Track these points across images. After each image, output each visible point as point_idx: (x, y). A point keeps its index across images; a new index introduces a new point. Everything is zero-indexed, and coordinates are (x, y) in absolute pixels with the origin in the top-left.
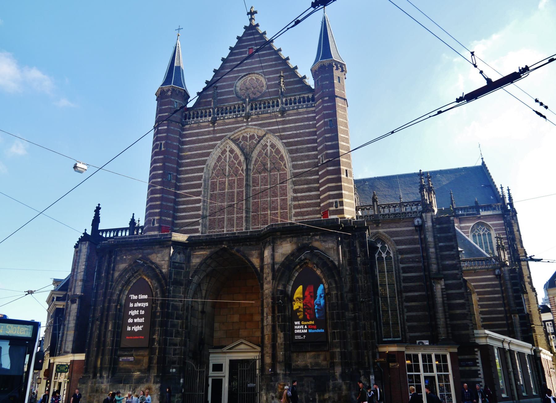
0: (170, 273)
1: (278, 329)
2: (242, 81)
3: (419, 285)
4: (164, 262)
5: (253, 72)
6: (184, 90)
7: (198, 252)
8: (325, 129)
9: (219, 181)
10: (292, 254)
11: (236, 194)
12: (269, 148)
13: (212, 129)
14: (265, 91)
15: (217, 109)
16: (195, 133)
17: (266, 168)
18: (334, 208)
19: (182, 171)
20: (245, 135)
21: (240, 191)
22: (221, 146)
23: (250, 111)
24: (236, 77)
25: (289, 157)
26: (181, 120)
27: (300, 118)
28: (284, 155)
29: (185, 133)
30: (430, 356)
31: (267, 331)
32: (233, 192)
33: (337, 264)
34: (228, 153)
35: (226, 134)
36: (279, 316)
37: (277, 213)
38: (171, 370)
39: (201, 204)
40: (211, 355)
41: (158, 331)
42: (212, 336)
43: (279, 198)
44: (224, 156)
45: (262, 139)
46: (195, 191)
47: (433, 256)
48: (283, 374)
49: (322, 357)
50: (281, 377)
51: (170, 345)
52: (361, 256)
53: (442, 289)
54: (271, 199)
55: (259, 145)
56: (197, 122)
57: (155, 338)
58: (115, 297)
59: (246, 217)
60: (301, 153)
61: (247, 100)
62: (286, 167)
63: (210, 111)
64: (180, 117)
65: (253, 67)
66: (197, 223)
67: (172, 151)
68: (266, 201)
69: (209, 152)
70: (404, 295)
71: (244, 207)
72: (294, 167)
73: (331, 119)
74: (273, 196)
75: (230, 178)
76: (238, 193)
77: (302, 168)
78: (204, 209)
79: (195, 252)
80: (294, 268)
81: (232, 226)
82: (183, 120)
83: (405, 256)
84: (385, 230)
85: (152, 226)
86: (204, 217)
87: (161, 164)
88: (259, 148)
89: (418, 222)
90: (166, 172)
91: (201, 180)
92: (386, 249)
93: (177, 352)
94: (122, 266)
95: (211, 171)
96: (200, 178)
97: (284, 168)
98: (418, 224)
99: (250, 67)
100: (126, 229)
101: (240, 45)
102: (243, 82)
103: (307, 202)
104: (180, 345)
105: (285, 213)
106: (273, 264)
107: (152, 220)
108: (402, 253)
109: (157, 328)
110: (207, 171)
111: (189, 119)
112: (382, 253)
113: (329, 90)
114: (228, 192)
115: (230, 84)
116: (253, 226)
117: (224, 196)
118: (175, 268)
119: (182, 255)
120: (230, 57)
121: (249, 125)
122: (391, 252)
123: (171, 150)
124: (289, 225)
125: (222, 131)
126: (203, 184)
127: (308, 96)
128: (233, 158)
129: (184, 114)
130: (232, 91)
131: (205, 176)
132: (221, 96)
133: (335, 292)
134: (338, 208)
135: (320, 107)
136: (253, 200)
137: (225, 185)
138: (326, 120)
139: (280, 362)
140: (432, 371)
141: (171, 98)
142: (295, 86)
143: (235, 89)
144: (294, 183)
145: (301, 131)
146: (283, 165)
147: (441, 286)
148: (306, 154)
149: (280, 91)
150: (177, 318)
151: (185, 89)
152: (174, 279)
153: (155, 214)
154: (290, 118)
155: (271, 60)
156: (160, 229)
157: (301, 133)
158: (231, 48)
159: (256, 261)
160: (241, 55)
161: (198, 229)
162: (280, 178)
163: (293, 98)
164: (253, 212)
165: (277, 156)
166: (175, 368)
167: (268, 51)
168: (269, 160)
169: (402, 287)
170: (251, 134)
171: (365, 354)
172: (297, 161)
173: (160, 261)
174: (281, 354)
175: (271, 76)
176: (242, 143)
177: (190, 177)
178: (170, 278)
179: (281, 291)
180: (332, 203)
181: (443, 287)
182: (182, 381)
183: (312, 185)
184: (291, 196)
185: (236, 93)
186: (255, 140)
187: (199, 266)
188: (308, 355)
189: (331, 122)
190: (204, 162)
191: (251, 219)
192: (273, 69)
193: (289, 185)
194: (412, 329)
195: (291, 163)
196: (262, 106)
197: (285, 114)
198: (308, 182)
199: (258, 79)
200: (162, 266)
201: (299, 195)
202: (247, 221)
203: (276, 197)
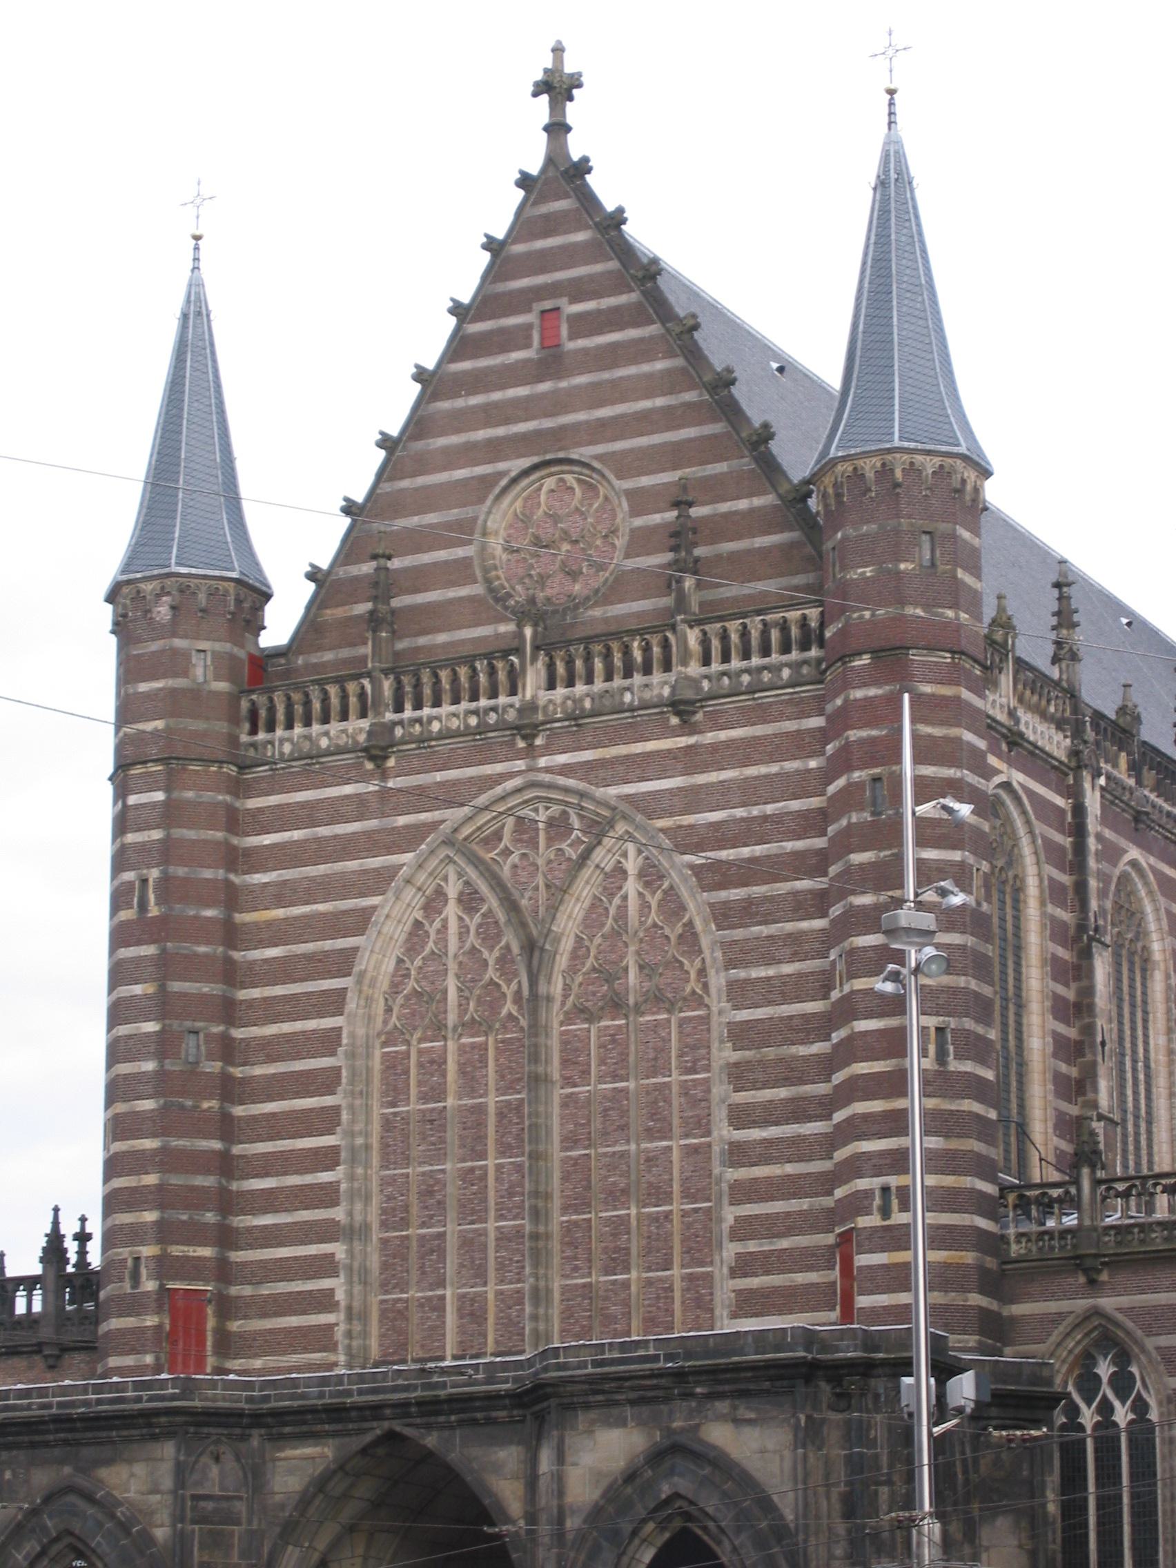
0: (181, 1539)
4: (158, 1497)
5: (561, 455)
7: (292, 1448)
9: (420, 1052)
11: (492, 1120)
12: (632, 886)
16: (303, 805)
20: (527, 812)
22: (421, 878)
23: (542, 693)
24: (486, 482)
26: (233, 740)
27: (765, 737)
28: (699, 925)
29: (253, 803)
32: (480, 1110)
34: (452, 910)
35: (436, 815)
37: (668, 1216)
44: (437, 924)
46: (311, 1110)
52: (896, 1478)
54: (643, 1146)
55: (586, 873)
60: (765, 923)
62: (705, 986)
64: (222, 727)
66: (326, 1267)
68: (623, 1155)
69: (364, 909)
73: (877, 770)
74: (650, 1134)
75: (464, 1040)
76: (501, 1115)
77: (770, 1003)
79: (281, 1449)
80: (635, 1533)
81: (480, 1275)
82: (244, 738)
84: (1125, 1301)
85: (129, 1291)
88: (585, 888)
91: (333, 1054)
95: (382, 1001)
96: (328, 1042)
99: (548, 423)
100: (29, 1283)
101: (502, 287)
103: (790, 1169)
105: (700, 1216)
107: (130, 1263)
110: (362, 1002)
111: (271, 728)
113: (873, 615)
117: (443, 1128)
118: (202, 1519)
121: (539, 770)
122: (1152, 1402)
123: (192, 913)
125: (421, 798)
126: (344, 1073)
128: (478, 933)
129: (245, 705)
130: (466, 563)
131: (352, 1035)
132: (416, 591)
138: (856, 775)
141: (174, 634)
143: (483, 548)
144: (739, 1076)
145: (769, 809)
146: (693, 975)
148: (790, 927)
153: (135, 1235)
154: (723, 735)
155: (650, 386)
157: (765, 818)
158: (457, 309)
161: (332, 1291)
164: (565, 1209)
165: (667, 931)
170: (555, 809)
172: (747, 964)
173: (143, 1494)
175: (645, 481)
176: (514, 858)
177: (289, 1038)
180: (868, 1194)
187: (295, 1508)
189: (878, 785)
190: (343, 963)
191: (556, 1245)
192: (657, 439)
195: (722, 974)
196: (598, 665)
197: (699, 716)
198: (792, 1073)
200: (153, 1513)
201: (756, 1134)
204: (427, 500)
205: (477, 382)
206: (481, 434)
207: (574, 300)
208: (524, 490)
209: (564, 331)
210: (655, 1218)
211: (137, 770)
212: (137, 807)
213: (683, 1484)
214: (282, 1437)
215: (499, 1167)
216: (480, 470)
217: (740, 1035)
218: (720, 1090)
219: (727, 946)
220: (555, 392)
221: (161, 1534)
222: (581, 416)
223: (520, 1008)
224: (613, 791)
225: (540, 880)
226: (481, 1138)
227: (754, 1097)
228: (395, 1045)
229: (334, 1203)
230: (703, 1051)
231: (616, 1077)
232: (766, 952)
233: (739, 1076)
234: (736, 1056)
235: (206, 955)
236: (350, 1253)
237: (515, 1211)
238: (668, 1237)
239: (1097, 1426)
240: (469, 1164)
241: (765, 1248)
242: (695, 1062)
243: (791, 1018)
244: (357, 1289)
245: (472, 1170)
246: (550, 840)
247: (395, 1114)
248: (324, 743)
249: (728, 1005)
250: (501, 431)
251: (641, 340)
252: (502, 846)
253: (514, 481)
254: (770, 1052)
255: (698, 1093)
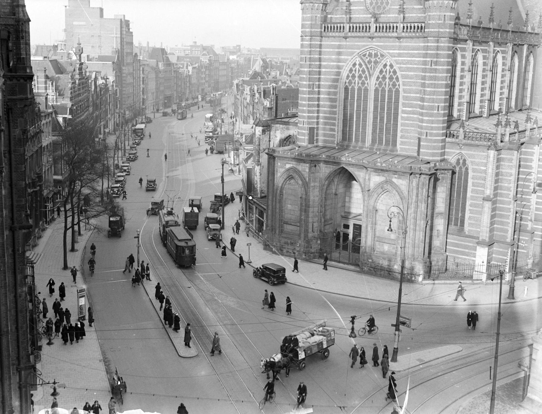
20: (371, 51)
28: (399, 76)
170: (376, 52)
229: (336, 108)
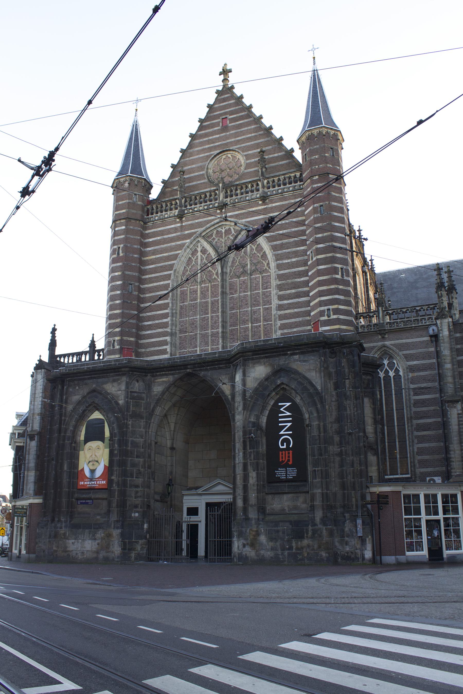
1: (250, 468)
2: (215, 161)
3: (434, 410)
4: (121, 392)
5: (228, 149)
6: (145, 179)
8: (314, 217)
9: (190, 289)
10: (267, 379)
11: (210, 305)
13: (179, 225)
14: (243, 171)
15: (184, 199)
16: (160, 231)
17: (246, 270)
18: (326, 318)
19: (146, 279)
20: (219, 229)
21: (215, 300)
25: (273, 255)
26: (143, 216)
27: (286, 204)
28: (267, 253)
29: (147, 232)
30: (435, 496)
31: (239, 470)
32: (207, 302)
33: (320, 389)
34: (199, 254)
35: (196, 230)
36: (251, 452)
37: (260, 326)
38: (133, 515)
39: (169, 319)
40: (185, 498)
41: (117, 472)
42: (186, 476)
43: (261, 307)
44: (195, 258)
45: (240, 234)
46: (162, 304)
47: (449, 374)
48: (255, 519)
49: (301, 499)
50: (253, 522)
51: (131, 486)
52: (350, 377)
53: (458, 414)
54: (252, 308)
56: (162, 217)
57: (114, 479)
58: (69, 434)
59: (223, 332)
60: (287, 249)
61: (221, 185)
62: (269, 268)
63: (176, 203)
64: (140, 212)
65: (227, 143)
66: (165, 343)
67: (132, 256)
68: (247, 311)
69: (176, 254)
70: (415, 422)
71: (220, 320)
72: (279, 267)
73: (321, 204)
74: (255, 305)
75: (203, 285)
76: (212, 303)
77: (289, 269)
78: (172, 325)
80: (269, 395)
81: (207, 344)
82: (145, 217)
83: (416, 374)
84: (393, 342)
85: (112, 349)
86: (172, 334)
87: (120, 273)
89: (433, 330)
90: (126, 282)
92: (394, 366)
93: (139, 494)
94: (76, 398)
95: (180, 277)
97: (267, 268)
98: (434, 333)
100: (86, 353)
101: (212, 114)
102: (216, 162)
103: (296, 310)
104: (142, 487)
106: (244, 391)
108: (414, 370)
109: (115, 468)
110: (175, 277)
112: (390, 371)
113: (318, 167)
114: (200, 303)
115: (201, 166)
116: (231, 343)
117: (196, 308)
118: (133, 398)
119: (141, 383)
120: (199, 131)
122: (401, 370)
123: (131, 255)
124: (262, 343)
125: (192, 227)
127: (295, 175)
128: (206, 259)
129: (146, 209)
130: (203, 174)
131: (173, 285)
132: (190, 183)
133: (317, 423)
134: (331, 318)
135: (309, 189)
136: (231, 311)
137: (197, 294)
138: (315, 205)
139: (252, 506)
140: (436, 513)
142: (281, 163)
143: (207, 172)
144: (280, 287)
146: (266, 265)
147: (458, 410)
148: (294, 249)
149: (260, 171)
150: (137, 457)
151: (145, 177)
152: (133, 411)
153: (115, 334)
154: (274, 205)
156: (121, 351)
157: (286, 223)
159: (226, 389)
160: (212, 128)
162: (262, 281)
163: (276, 179)
165: (258, 254)
166: (138, 512)
167: (246, 120)
168: (249, 260)
169: (412, 412)
171: (353, 495)
172: (282, 259)
173: (116, 391)
174: (253, 496)
175: (250, 152)
176: (216, 240)
177: (155, 287)
178: (128, 410)
179: (254, 423)
180: (324, 311)
181: (460, 412)
182: (146, 526)
183: (301, 289)
184: (276, 304)
185: (208, 177)
186: (231, 236)
187: (160, 395)
188: (285, 497)
189: (321, 207)
190: (171, 267)
192: (253, 143)
193: (273, 291)
194: (423, 463)
195: (275, 262)
197: (267, 201)
198: (296, 285)
199: (235, 157)
200: (119, 396)
201: (286, 302)
202: (223, 338)
203: (258, 306)
204: (193, 162)
205: (206, 135)
206: (207, 146)
207: (230, 115)
208: (217, 159)
209: (228, 122)
210: (256, 327)
211: (118, 222)
212: (118, 230)
213: (285, 380)
214: (157, 376)
215: (212, 317)
216: (206, 154)
217: (280, 277)
218: (274, 292)
219: (275, 255)
220: (225, 135)
221: (121, 402)
222: (233, 140)
223: (218, 277)
224: (244, 220)
225: (223, 245)
226: (207, 309)
227: (285, 292)
228: (184, 288)
230: (269, 284)
231: (245, 292)
232: (288, 256)
233: (280, 287)
234: (279, 283)
235: (134, 266)
236: (171, 339)
237: (216, 327)
238: (260, 331)
239: (384, 377)
240: (204, 316)
241: (290, 331)
242: (267, 286)
243: (295, 272)
244: (173, 349)
245: (205, 317)
246: (225, 235)
247: (184, 305)
248: (166, 216)
249: (277, 270)
250: (212, 145)
251: (248, 122)
252: (213, 237)
253: (215, 156)
254: (290, 281)
255: (268, 294)
